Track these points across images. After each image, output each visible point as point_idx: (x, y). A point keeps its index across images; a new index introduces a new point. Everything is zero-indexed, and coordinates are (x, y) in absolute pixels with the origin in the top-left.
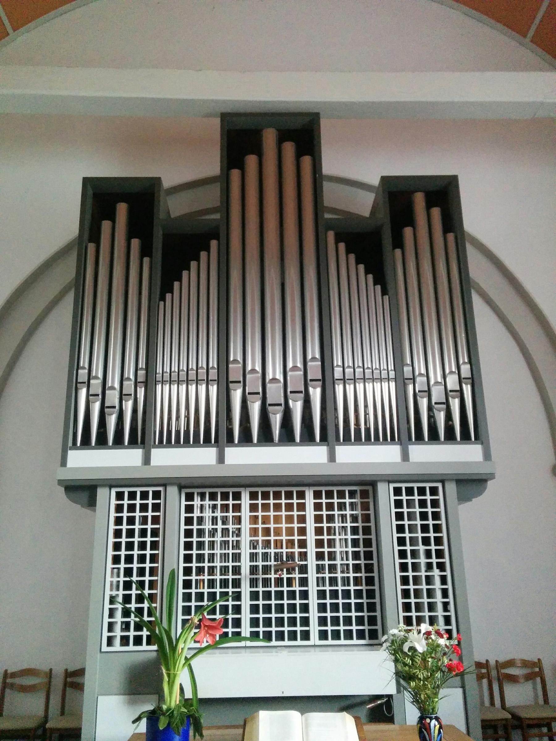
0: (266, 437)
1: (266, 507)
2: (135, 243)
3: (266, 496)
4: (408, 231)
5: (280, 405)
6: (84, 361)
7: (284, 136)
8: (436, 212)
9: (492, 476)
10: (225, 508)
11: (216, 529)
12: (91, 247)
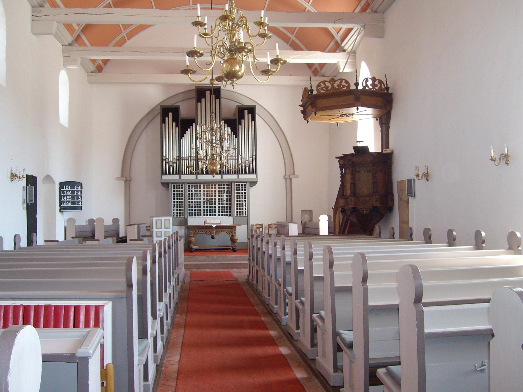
2: (174, 123)
3: (207, 186)
4: (243, 121)
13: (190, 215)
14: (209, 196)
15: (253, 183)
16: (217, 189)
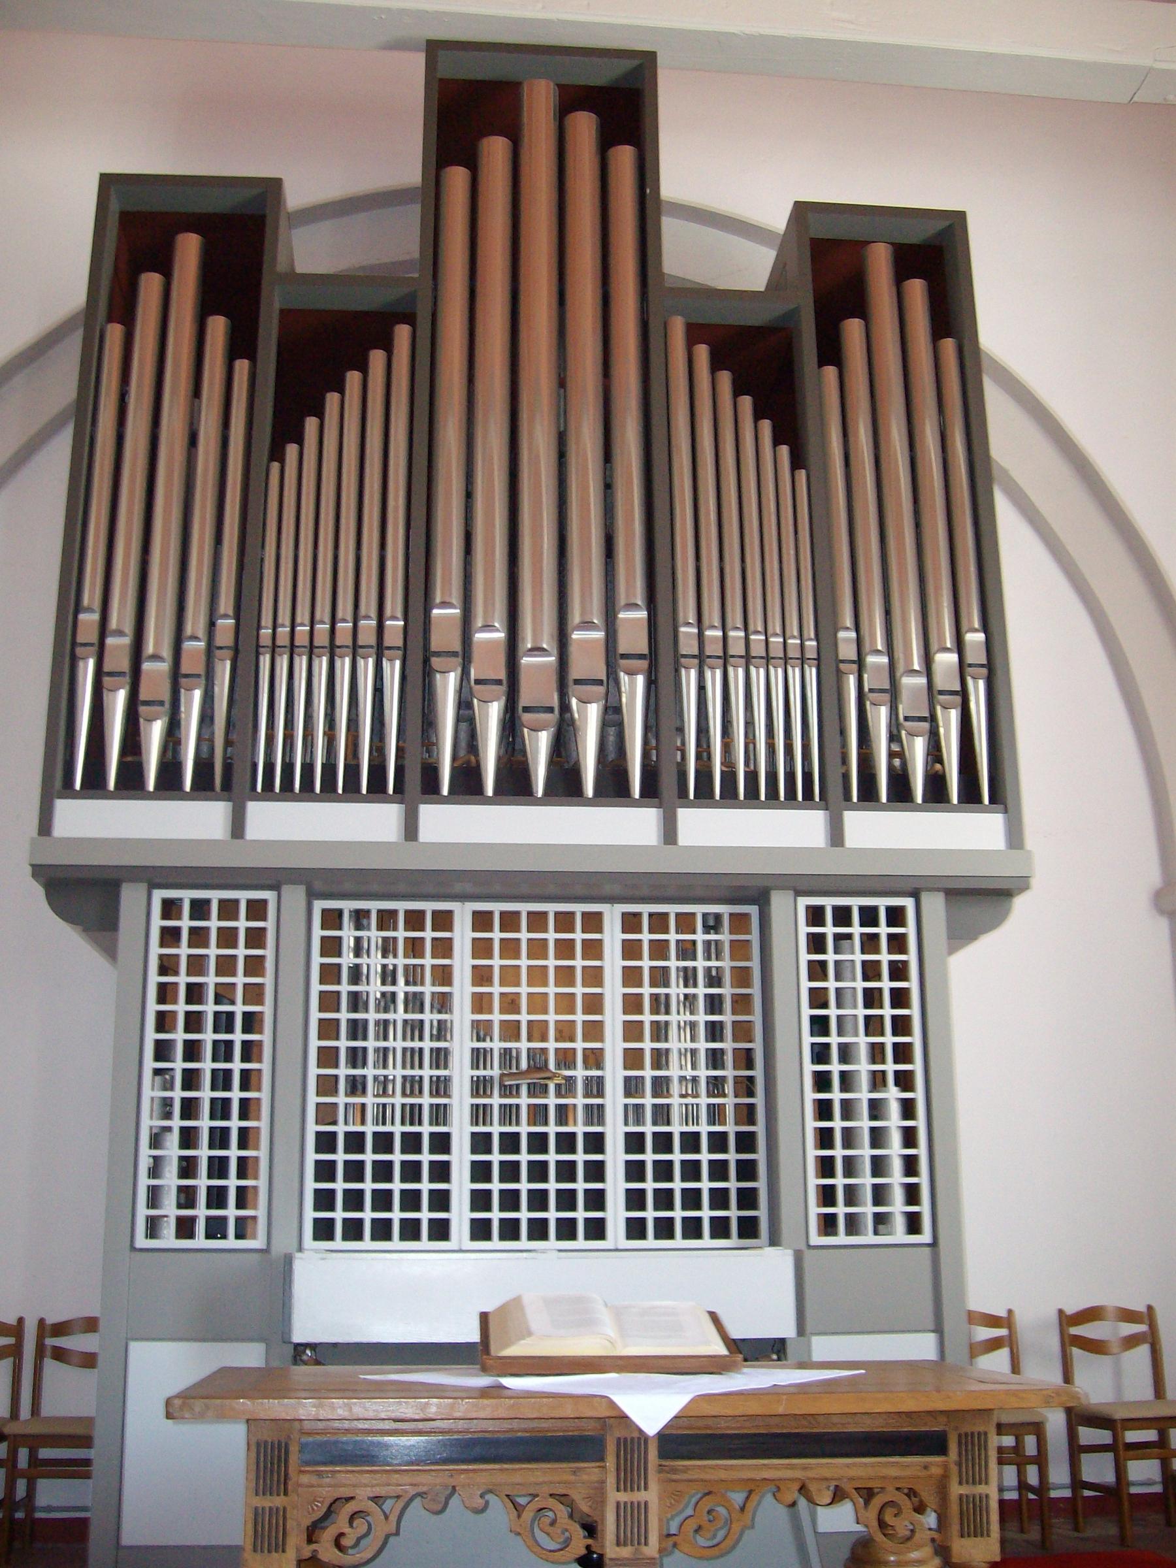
0: (515, 784)
1: (510, 948)
2: (218, 326)
4: (853, 328)
5: (550, 710)
6: (91, 595)
7: (572, 99)
8: (917, 288)
9: (1021, 884)
10: (414, 948)
11: (394, 994)
12: (115, 332)
13: (324, 1230)
14: (538, 1031)
15: (980, 899)
16: (613, 962)
